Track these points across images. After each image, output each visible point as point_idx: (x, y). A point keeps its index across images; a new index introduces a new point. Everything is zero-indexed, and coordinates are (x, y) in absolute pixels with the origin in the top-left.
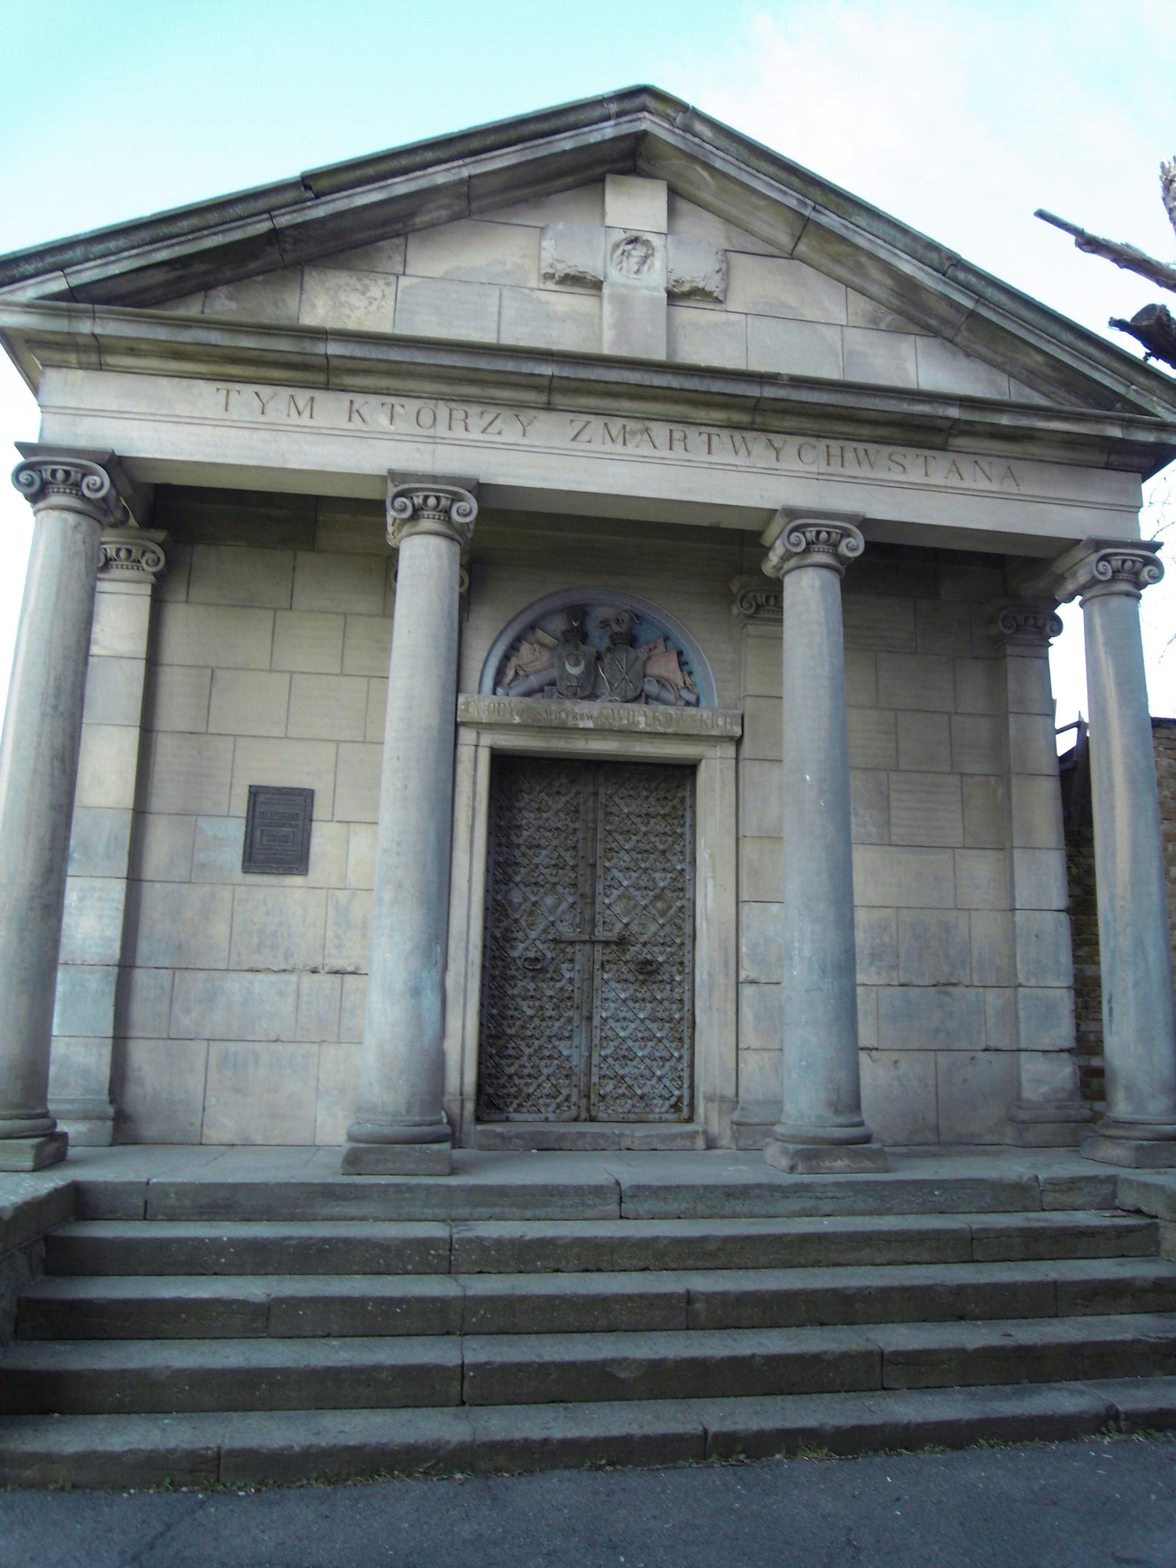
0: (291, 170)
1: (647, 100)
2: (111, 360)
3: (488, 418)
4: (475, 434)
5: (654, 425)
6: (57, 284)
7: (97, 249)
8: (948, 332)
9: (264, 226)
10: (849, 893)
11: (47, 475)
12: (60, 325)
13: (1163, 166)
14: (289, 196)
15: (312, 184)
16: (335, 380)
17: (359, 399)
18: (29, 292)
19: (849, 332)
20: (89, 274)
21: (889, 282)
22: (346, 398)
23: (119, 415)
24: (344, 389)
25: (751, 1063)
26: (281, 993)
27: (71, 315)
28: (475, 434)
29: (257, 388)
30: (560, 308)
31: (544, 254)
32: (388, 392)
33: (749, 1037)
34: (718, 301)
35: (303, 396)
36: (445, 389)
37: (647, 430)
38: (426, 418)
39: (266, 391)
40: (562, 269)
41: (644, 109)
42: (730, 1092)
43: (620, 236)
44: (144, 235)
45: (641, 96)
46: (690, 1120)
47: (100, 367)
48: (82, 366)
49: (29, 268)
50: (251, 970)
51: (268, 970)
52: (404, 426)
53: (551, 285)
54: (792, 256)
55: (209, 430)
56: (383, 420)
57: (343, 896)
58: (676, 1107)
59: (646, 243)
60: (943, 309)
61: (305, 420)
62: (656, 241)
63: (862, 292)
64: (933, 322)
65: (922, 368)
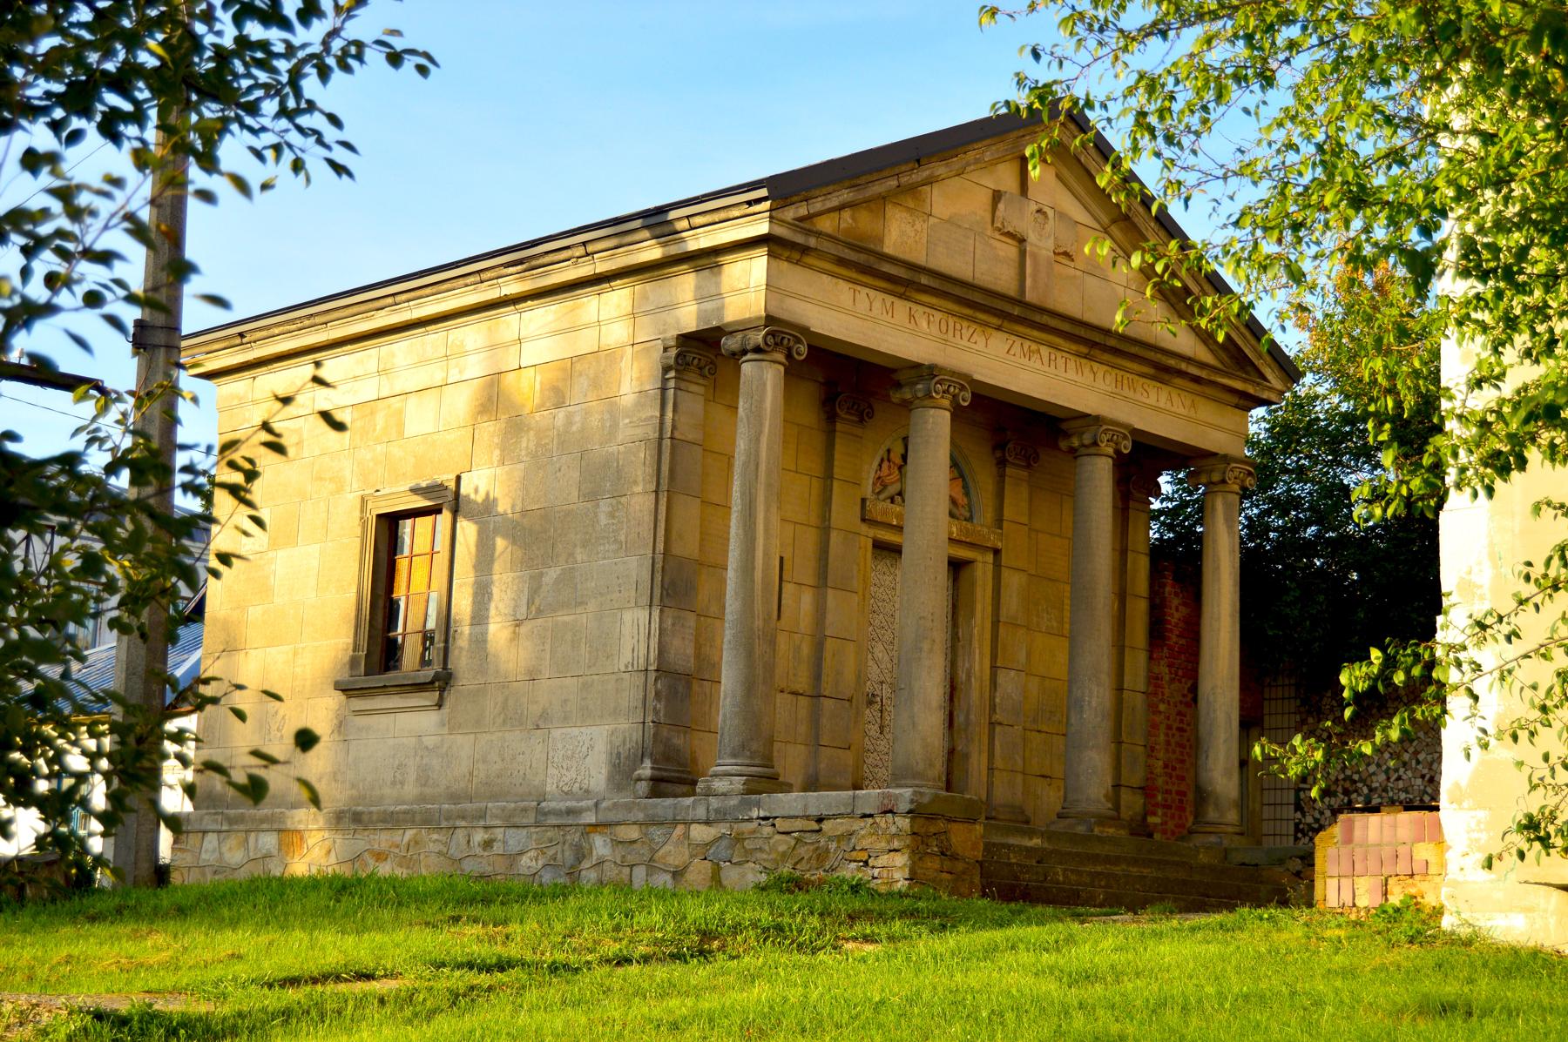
4: (964, 342)
22: (909, 304)
23: (804, 298)
28: (964, 342)
29: (867, 290)
30: (1002, 254)
33: (998, 763)
35: (889, 299)
38: (944, 329)
39: (872, 293)
48: (788, 260)
52: (934, 329)
56: (925, 324)
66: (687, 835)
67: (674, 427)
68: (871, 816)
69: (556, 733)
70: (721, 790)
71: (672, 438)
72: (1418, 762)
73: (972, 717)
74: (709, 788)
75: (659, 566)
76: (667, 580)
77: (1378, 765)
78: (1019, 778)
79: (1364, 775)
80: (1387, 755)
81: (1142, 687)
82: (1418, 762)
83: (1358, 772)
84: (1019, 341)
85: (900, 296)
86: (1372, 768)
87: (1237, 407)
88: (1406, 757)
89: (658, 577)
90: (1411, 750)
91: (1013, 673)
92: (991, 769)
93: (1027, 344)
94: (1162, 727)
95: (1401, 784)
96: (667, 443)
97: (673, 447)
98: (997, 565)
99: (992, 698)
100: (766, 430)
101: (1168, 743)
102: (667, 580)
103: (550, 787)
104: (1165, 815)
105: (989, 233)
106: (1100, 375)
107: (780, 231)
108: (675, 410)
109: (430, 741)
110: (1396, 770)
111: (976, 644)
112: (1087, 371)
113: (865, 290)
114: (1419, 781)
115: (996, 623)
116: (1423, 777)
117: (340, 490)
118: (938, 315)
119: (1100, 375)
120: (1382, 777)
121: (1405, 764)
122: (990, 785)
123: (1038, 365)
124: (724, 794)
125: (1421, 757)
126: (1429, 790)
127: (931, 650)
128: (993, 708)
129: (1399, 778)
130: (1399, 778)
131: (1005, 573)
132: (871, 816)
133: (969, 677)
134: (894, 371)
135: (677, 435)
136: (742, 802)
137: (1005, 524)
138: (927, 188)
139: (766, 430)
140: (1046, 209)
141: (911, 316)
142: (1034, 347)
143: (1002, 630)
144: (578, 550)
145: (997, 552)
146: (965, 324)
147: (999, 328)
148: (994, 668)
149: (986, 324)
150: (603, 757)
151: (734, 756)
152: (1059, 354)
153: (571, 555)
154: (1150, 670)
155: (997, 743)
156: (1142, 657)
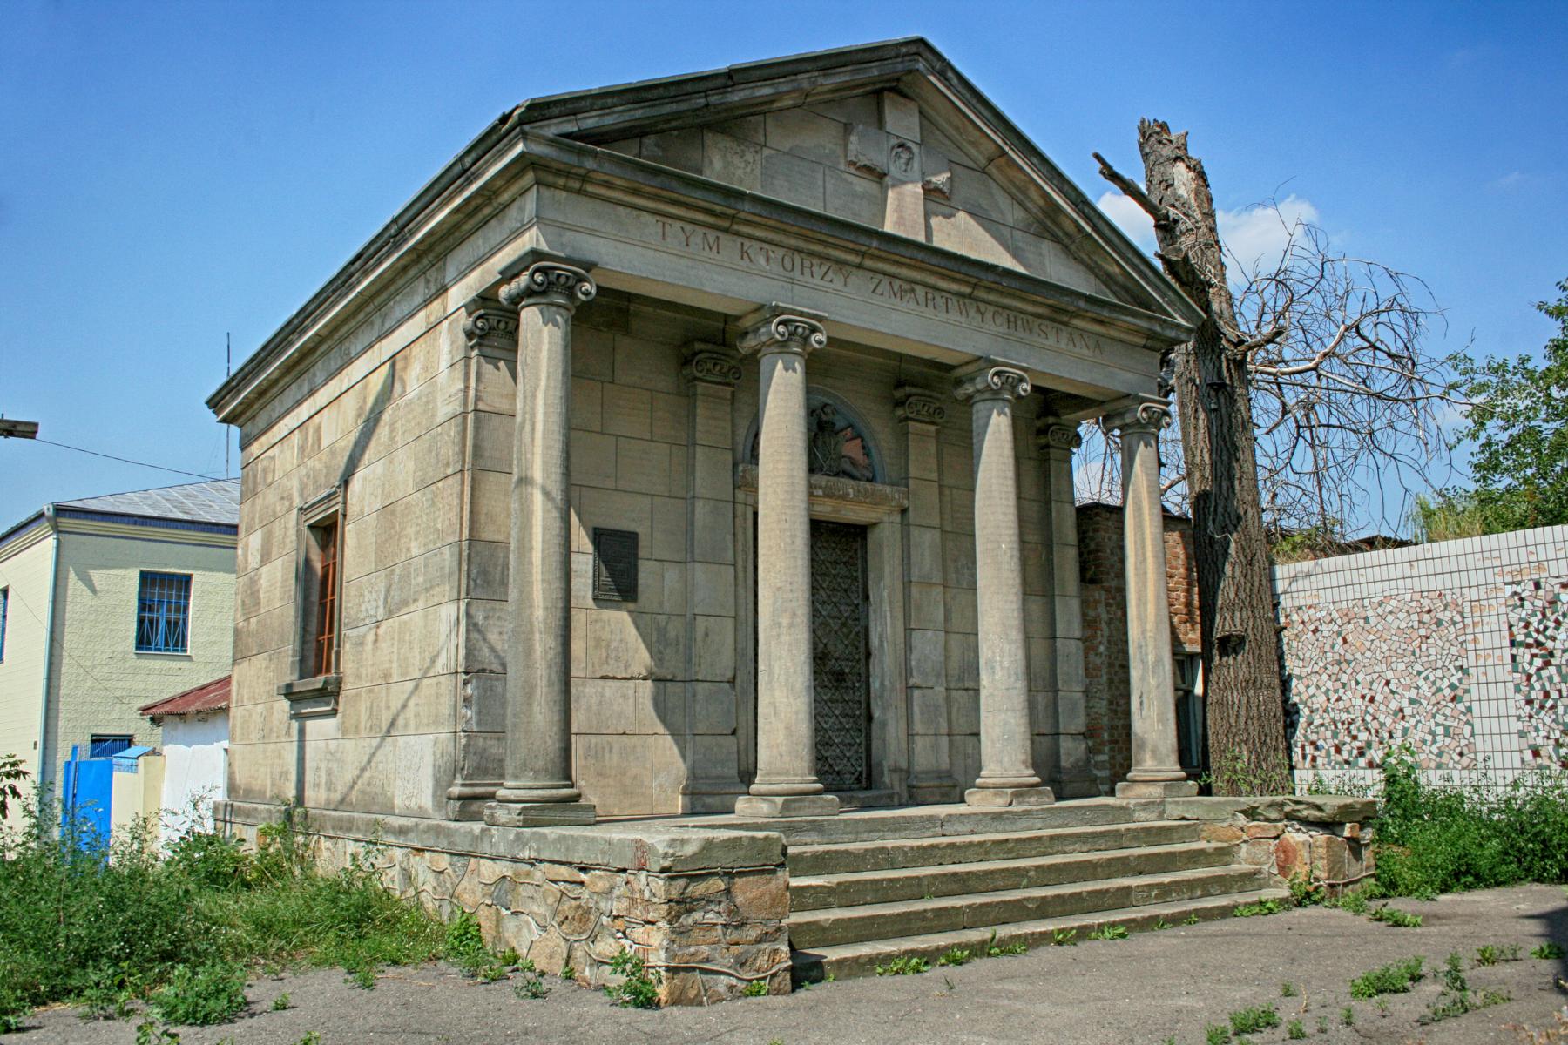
0: (722, 65)
1: (922, 49)
2: (590, 188)
3: (824, 269)
4: (817, 280)
5: (917, 287)
6: (570, 127)
7: (600, 102)
8: (1066, 240)
9: (702, 101)
10: (1053, 630)
11: (553, 278)
12: (571, 159)
13: (1143, 122)
14: (719, 82)
15: (733, 77)
16: (735, 227)
17: (747, 243)
18: (552, 129)
19: (1016, 232)
20: (590, 122)
21: (1041, 202)
22: (740, 240)
23: (591, 232)
24: (737, 234)
25: (920, 744)
26: (625, 697)
27: (581, 152)
28: (817, 280)
30: (858, 189)
31: (851, 147)
32: (770, 243)
33: (918, 727)
34: (948, 199)
35: (712, 235)
36: (802, 244)
37: (913, 290)
38: (788, 265)
40: (863, 161)
41: (918, 54)
42: (904, 765)
43: (894, 141)
44: (630, 96)
45: (921, 46)
46: (869, 787)
47: (579, 192)
48: (565, 188)
49: (556, 111)
50: (602, 678)
51: (614, 678)
52: (775, 267)
53: (852, 170)
54: (983, 172)
55: (652, 253)
56: (762, 261)
57: (662, 619)
58: (858, 780)
59: (909, 149)
60: (1071, 229)
61: (713, 254)
62: (915, 149)
63: (1021, 204)
64: (1060, 233)
65: (1058, 270)
66: (476, 872)
67: (478, 399)
68: (624, 870)
69: (401, 740)
70: (503, 820)
71: (476, 410)
72: (1357, 683)
73: (887, 683)
74: (492, 815)
75: (465, 554)
76: (474, 572)
77: (1318, 687)
78: (945, 740)
79: (1304, 697)
80: (1325, 677)
81: (1078, 634)
82: (1357, 683)
83: (1299, 694)
84: (886, 281)
85: (727, 231)
86: (1312, 690)
87: (1145, 347)
88: (1344, 678)
89: (464, 567)
90: (1349, 671)
91: (930, 634)
92: (910, 735)
93: (897, 283)
94: (1105, 670)
95: (1341, 705)
96: (470, 417)
97: (477, 420)
98: (905, 526)
99: (907, 661)
100: (543, 383)
101: (1111, 681)
102: (474, 572)
103: (397, 802)
104: (1112, 750)
105: (842, 167)
106: (988, 316)
107: (539, 149)
108: (478, 380)
109: (332, 745)
110: (1336, 691)
111: (886, 607)
112: (972, 312)
113: (678, 224)
114: (1360, 701)
115: (907, 584)
116: (1363, 697)
117: (289, 510)
118: (780, 252)
119: (988, 316)
120: (1323, 698)
121: (1344, 685)
122: (910, 753)
123: (913, 305)
124: (503, 825)
125: (1360, 677)
126: (1370, 710)
127: (791, 625)
128: (908, 672)
129: (1339, 699)
130: (1339, 699)
131: (915, 532)
132: (624, 870)
133: (881, 641)
134: (738, 318)
135: (481, 406)
136: (518, 835)
137: (911, 482)
138: (760, 118)
139: (543, 383)
140: (909, 144)
141: (743, 253)
142: (906, 286)
143: (915, 590)
144: (413, 544)
145: (904, 511)
146: (816, 261)
147: (859, 267)
148: (908, 630)
149: (842, 263)
150: (430, 770)
151: (516, 777)
152: (937, 295)
153: (408, 550)
154: (1084, 615)
155: (916, 709)
156: (1075, 604)
